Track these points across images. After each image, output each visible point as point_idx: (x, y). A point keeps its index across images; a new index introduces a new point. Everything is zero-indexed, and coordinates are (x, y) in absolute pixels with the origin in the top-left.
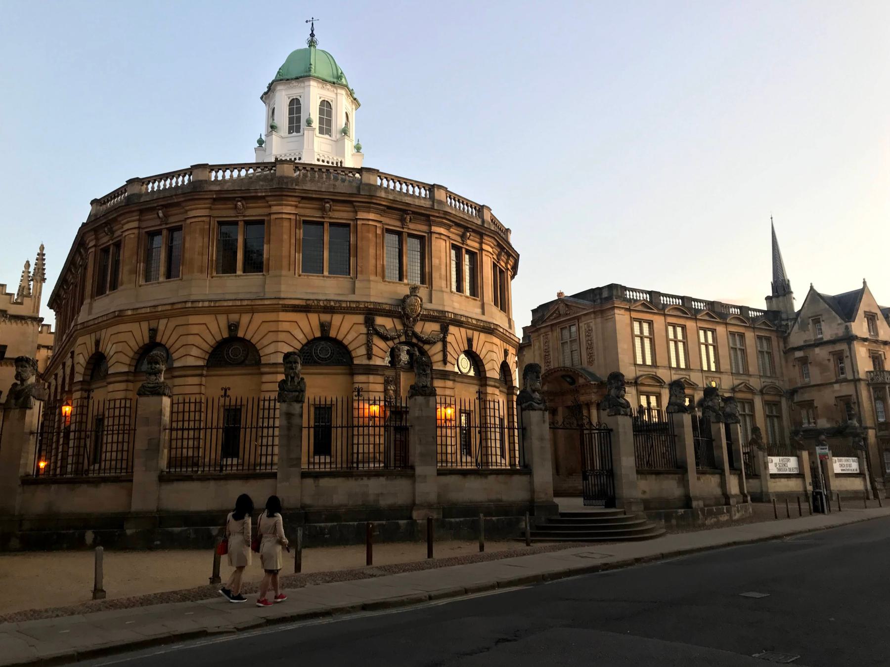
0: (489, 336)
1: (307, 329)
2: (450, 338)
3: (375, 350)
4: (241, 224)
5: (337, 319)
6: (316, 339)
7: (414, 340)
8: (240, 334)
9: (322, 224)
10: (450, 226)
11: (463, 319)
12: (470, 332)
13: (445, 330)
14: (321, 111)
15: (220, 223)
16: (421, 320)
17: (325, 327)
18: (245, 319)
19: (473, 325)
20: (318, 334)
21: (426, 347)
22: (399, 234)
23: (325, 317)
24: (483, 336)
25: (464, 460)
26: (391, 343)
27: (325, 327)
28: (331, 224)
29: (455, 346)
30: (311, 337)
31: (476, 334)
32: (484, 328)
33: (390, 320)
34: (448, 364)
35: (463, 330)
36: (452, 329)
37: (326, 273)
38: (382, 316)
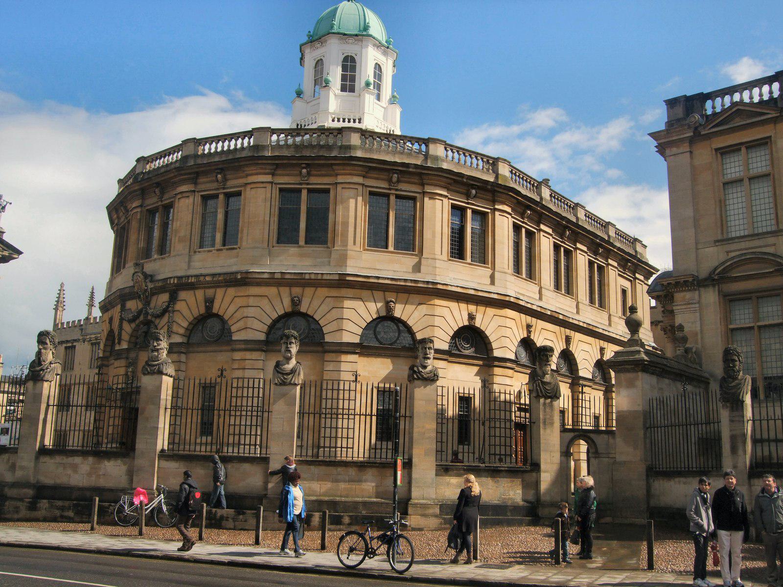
0: (243, 288)
2: (179, 306)
3: (123, 333)
7: (149, 317)
10: (197, 178)
11: (193, 280)
12: (210, 292)
13: (173, 299)
16: (153, 294)
19: (208, 282)
21: (157, 321)
24: (232, 291)
25: (198, 441)
26: (133, 325)
29: (186, 312)
31: (220, 292)
32: (226, 281)
33: (134, 301)
34: (173, 336)
35: (200, 294)
36: (183, 295)
38: (129, 299)
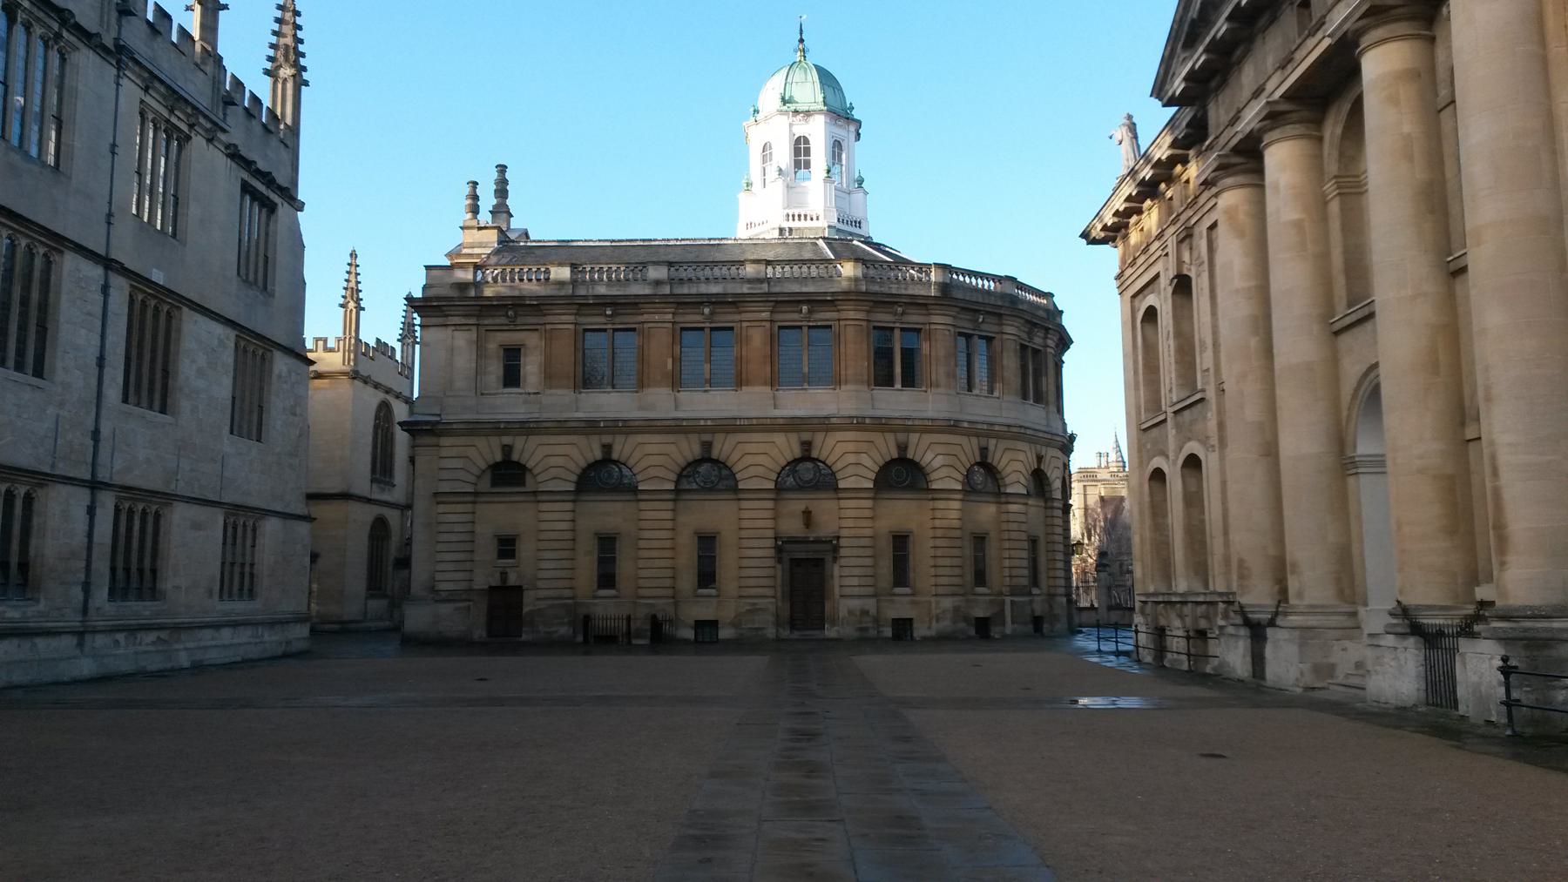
1: (884, 451)
4: (805, 330)
5: (914, 437)
6: (893, 460)
8: (814, 454)
9: (892, 329)
14: (797, 152)
15: (780, 328)
17: (902, 448)
18: (819, 437)
20: (895, 455)
22: (968, 337)
23: (902, 437)
27: (902, 448)
28: (902, 329)
30: (888, 459)
37: (898, 386)
